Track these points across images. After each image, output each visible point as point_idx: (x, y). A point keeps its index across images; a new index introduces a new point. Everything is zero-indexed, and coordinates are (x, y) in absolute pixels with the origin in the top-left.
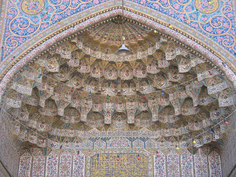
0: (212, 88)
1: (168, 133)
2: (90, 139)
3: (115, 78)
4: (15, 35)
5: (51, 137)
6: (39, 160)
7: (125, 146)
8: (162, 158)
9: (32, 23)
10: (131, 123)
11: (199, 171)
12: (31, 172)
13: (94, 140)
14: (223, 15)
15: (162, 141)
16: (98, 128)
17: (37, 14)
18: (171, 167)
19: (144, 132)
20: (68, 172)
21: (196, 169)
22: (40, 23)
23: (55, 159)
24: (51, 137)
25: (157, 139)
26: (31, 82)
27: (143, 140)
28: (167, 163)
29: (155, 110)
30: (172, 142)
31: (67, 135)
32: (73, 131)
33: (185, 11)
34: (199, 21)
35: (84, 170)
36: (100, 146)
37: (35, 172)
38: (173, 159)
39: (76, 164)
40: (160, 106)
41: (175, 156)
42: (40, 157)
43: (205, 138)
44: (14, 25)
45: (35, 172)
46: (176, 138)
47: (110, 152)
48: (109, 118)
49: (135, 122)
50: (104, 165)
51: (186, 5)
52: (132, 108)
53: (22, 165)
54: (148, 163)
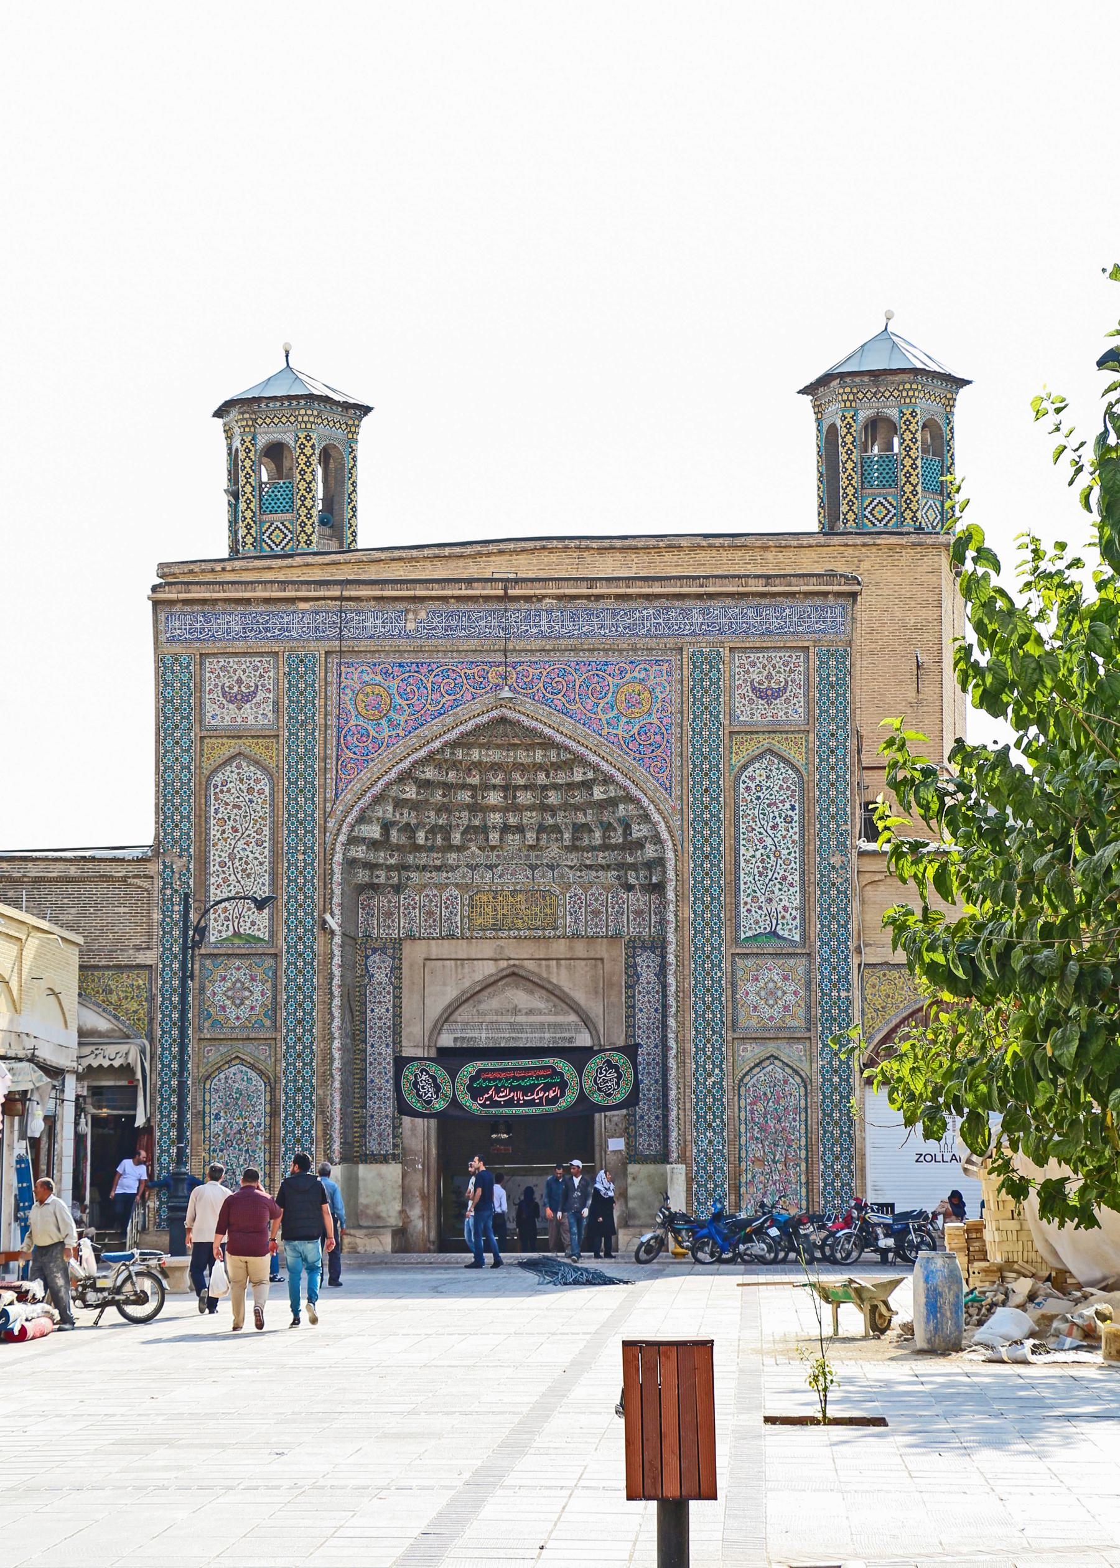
0: (637, 828)
1: (589, 858)
2: (467, 866)
3: (503, 783)
4: (352, 756)
5: (406, 867)
6: (389, 902)
7: (523, 877)
8: (580, 899)
9: (376, 735)
10: (531, 843)
11: (635, 919)
12: (378, 920)
13: (473, 868)
14: (655, 721)
15: (581, 871)
16: (479, 848)
17: (382, 718)
18: (593, 912)
19: (553, 854)
20: (434, 921)
21: (631, 915)
22: (386, 733)
23: (413, 899)
24: (406, 867)
25: (571, 868)
26: (378, 819)
27: (552, 867)
28: (587, 906)
29: (567, 828)
30: (597, 871)
31: (431, 863)
32: (440, 855)
33: (600, 713)
34: (620, 732)
35: (458, 918)
36: (482, 877)
37: (385, 921)
38: (596, 900)
39: (447, 908)
40: (574, 824)
41: (600, 894)
42: (389, 896)
43: (642, 873)
44: (349, 738)
45: (385, 921)
46: (602, 866)
47: (500, 888)
48: (497, 836)
49: (538, 839)
50: (489, 910)
51: (602, 703)
52: (532, 821)
53: (363, 909)
54: (559, 905)
